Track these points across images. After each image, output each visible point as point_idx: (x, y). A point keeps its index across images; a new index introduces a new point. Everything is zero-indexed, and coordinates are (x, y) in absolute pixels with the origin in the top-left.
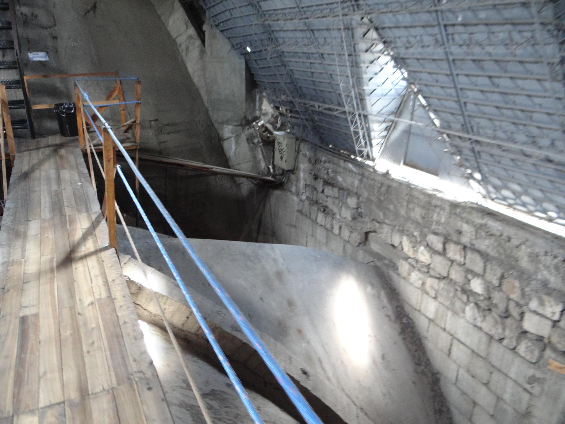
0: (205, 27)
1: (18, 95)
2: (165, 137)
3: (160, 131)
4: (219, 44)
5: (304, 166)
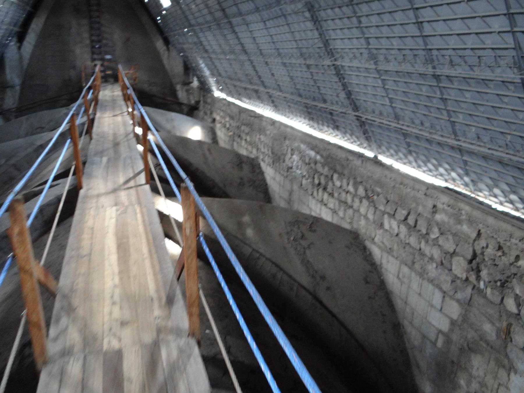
1: (102, 69)
4: (174, 53)
5: (202, 98)
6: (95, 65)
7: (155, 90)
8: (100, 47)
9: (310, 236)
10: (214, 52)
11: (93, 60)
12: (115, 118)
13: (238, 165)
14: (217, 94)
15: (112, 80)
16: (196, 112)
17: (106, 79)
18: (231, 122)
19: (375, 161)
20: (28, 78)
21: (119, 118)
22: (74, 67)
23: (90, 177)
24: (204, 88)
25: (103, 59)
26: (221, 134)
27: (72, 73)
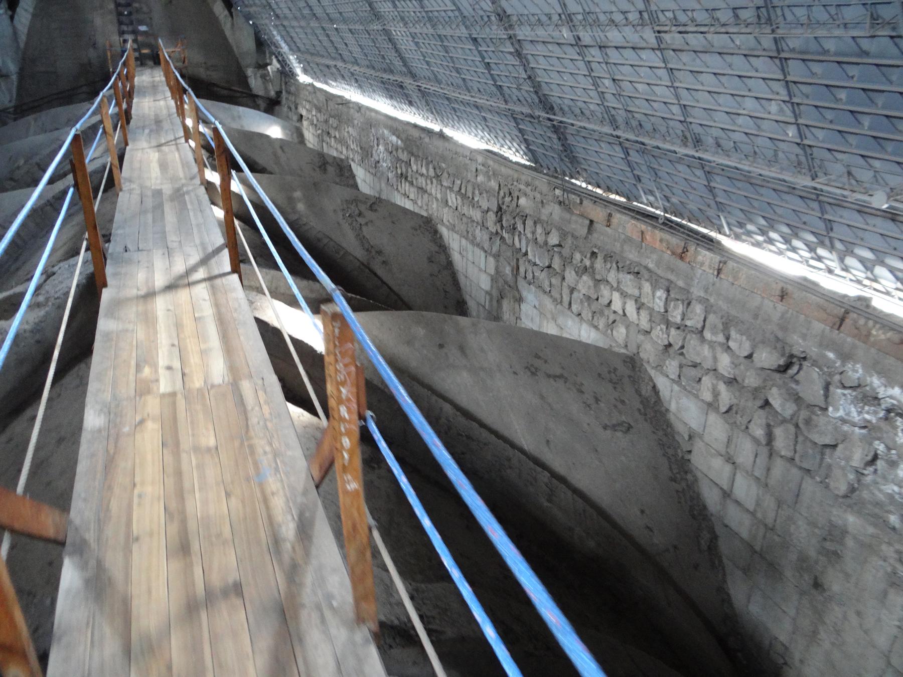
0: (233, 10)
1: (135, 46)
2: (208, 73)
3: (207, 69)
5: (283, 87)
6: (125, 41)
7: (215, 76)
8: (130, 14)
9: (370, 215)
10: (286, 18)
11: (122, 33)
12: (154, 97)
13: (320, 167)
14: (303, 78)
15: (151, 63)
16: (277, 108)
18: (319, 115)
19: (441, 135)
21: (162, 103)
23: (134, 140)
24: (286, 74)
25: (135, 32)
26: (310, 136)
27: (92, 54)
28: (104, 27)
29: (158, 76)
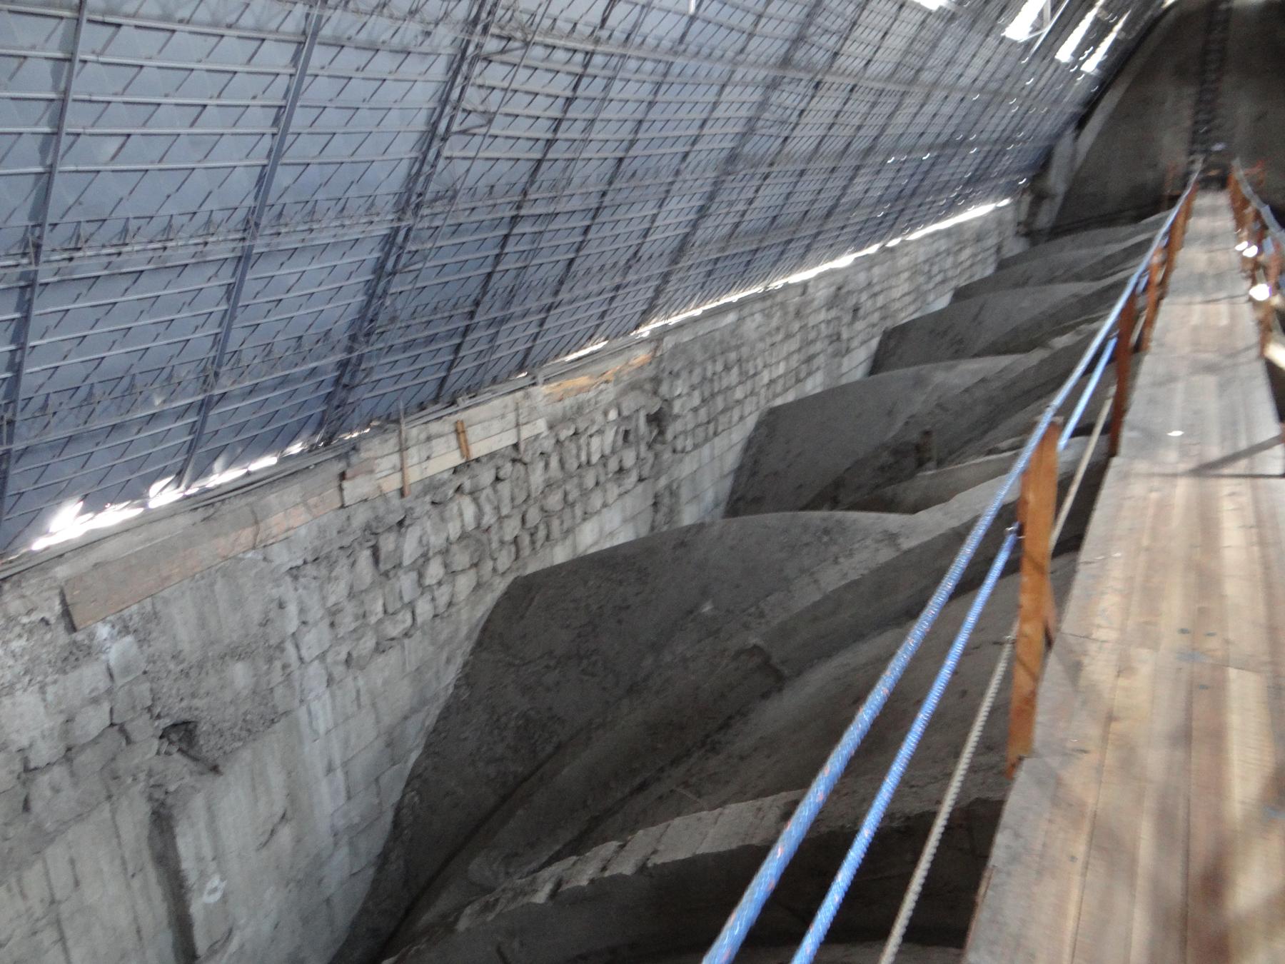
6: (1193, 162)
11: (1191, 153)
17: (1206, 184)
20: (1077, 183)
22: (1154, 166)
25: (1207, 152)
27: (1150, 176)
28: (1171, 147)
29: (1222, 199)
